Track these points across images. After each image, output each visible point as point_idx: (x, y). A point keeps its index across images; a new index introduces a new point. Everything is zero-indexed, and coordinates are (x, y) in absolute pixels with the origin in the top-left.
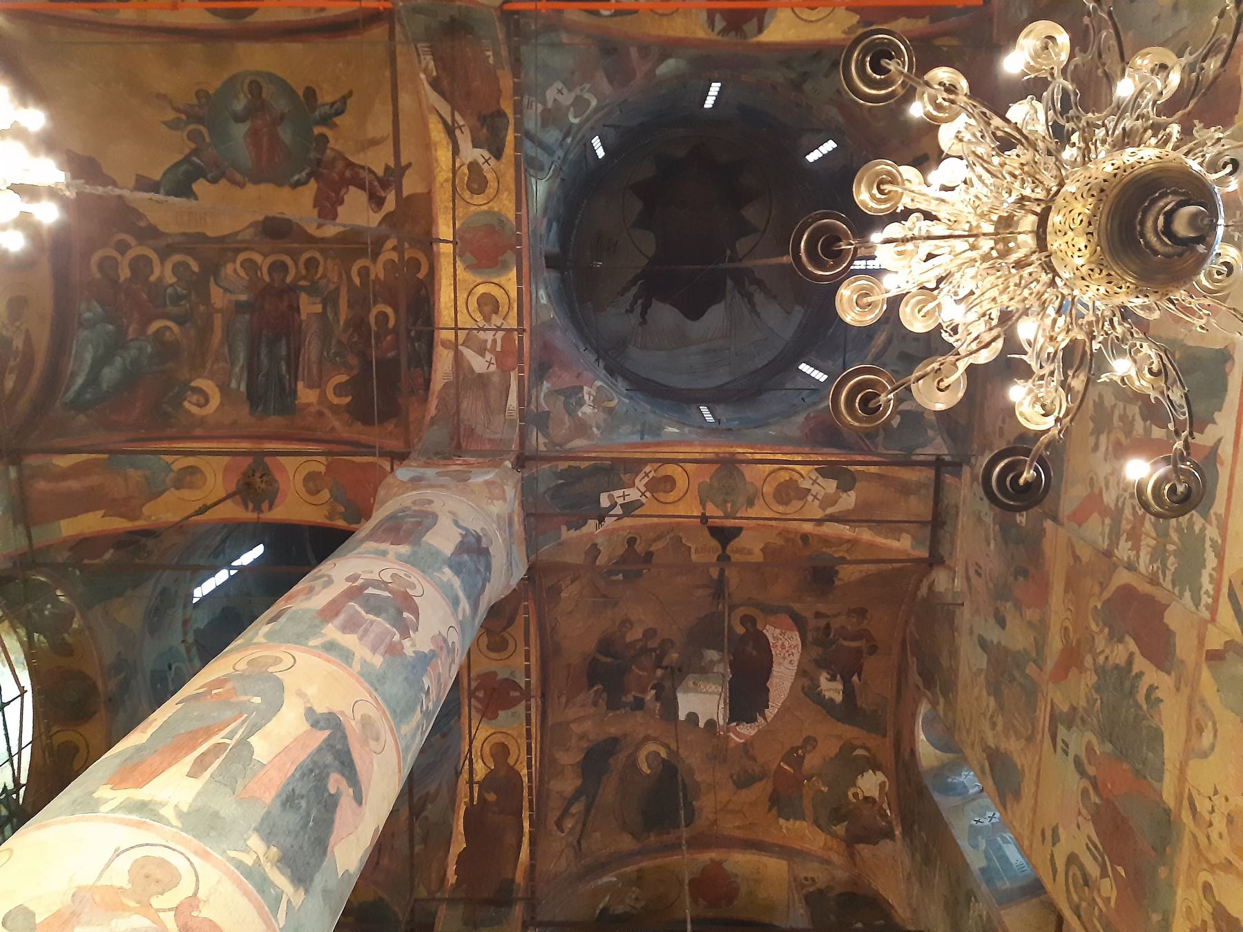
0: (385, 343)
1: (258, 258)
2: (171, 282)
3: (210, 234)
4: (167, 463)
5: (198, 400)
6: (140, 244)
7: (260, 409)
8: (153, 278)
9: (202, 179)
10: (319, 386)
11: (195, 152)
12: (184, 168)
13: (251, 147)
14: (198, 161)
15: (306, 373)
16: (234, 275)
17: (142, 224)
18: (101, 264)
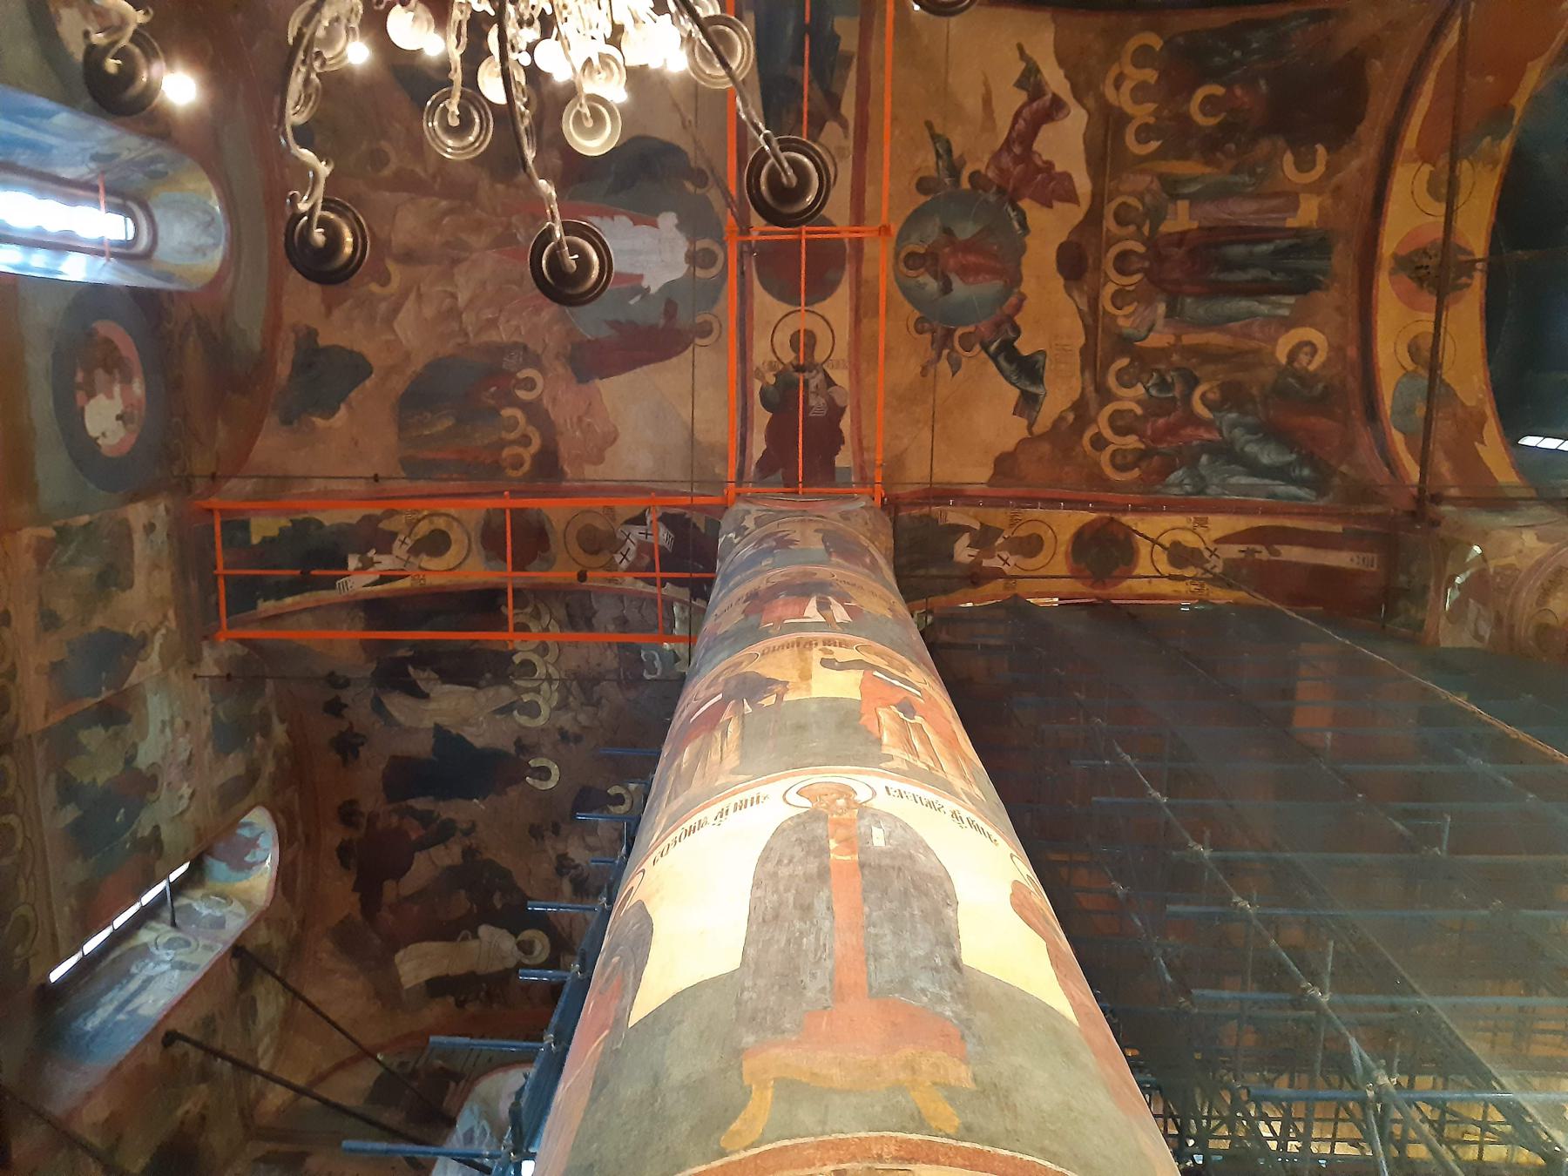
0: (1246, 99)
1: (1110, 289)
2: (1143, 390)
3: (1082, 341)
4: (1404, 375)
5: (1306, 354)
6: (1094, 421)
7: (1321, 278)
8: (1139, 411)
9: (1016, 344)
10: (1297, 195)
11: (985, 348)
12: (1004, 364)
13: (980, 278)
14: (995, 344)
15: (1274, 216)
16: (1132, 319)
17: (1071, 417)
18: (1118, 468)
